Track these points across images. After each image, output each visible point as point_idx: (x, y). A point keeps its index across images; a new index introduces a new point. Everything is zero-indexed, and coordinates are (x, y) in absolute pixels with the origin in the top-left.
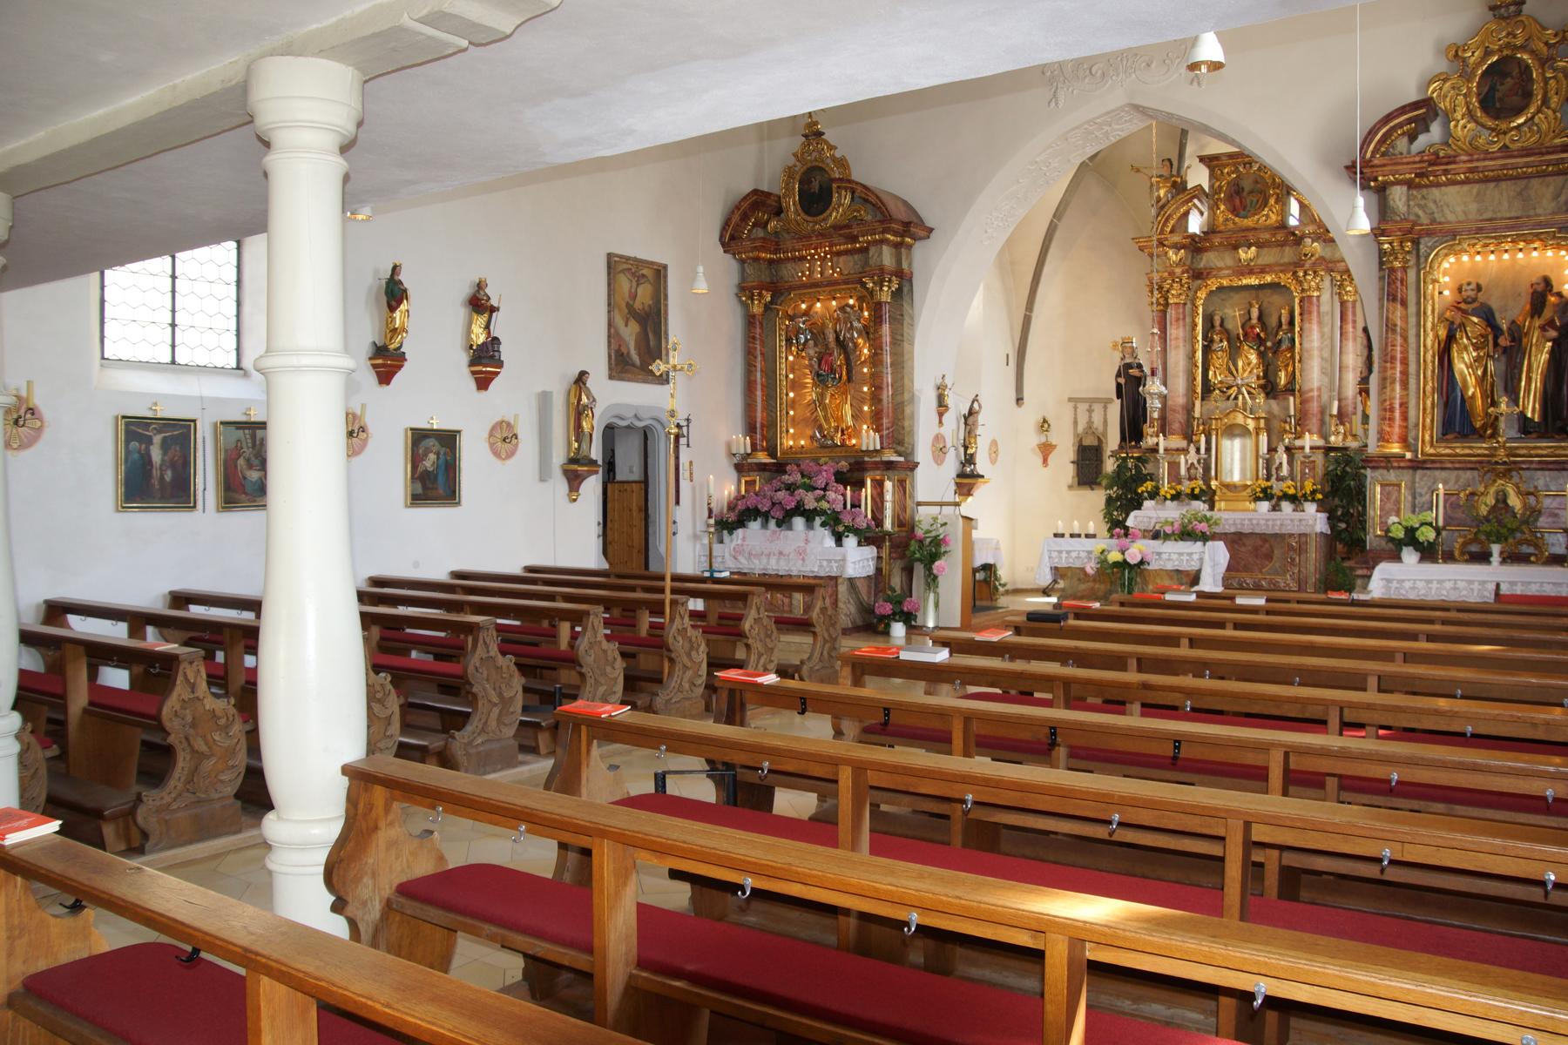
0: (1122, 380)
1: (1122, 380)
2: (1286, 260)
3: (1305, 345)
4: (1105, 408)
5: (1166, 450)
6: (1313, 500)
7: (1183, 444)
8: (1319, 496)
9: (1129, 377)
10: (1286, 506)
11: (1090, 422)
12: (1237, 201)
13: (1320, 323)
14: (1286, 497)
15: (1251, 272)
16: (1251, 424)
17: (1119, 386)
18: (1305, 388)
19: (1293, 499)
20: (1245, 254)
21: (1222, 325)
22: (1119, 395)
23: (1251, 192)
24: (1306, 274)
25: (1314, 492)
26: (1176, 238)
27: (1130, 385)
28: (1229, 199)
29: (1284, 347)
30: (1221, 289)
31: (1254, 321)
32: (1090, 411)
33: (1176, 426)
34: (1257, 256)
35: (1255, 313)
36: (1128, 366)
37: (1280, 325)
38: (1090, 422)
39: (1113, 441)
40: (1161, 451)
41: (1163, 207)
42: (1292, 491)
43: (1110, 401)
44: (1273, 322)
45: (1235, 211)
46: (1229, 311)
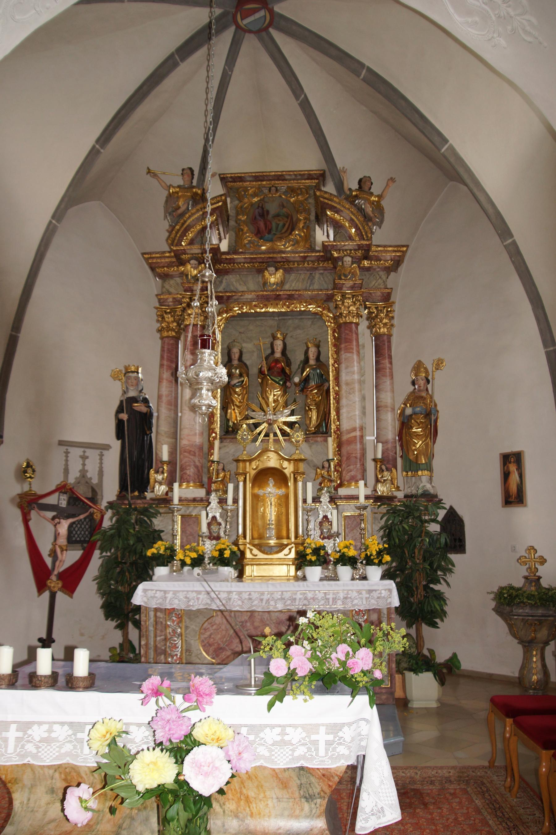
0: (124, 416)
1: (124, 416)
2: (316, 286)
3: (344, 377)
4: (101, 455)
5: (180, 500)
6: (380, 563)
7: (201, 493)
8: (387, 558)
9: (133, 413)
10: (345, 571)
11: (83, 473)
12: (262, 224)
13: (358, 352)
14: (345, 560)
15: (278, 298)
16: (288, 468)
17: (120, 424)
18: (345, 425)
19: (351, 562)
20: (274, 278)
21: (240, 359)
22: (120, 435)
23: (277, 215)
24: (344, 296)
25: (380, 553)
26: (196, 250)
27: (135, 425)
28: (254, 220)
29: (312, 383)
30: (243, 315)
31: (278, 355)
32: (84, 458)
33: (191, 471)
34: (282, 283)
35: (279, 345)
36: (133, 400)
37: (306, 360)
38: (83, 473)
39: (110, 490)
40: (176, 501)
41: (182, 215)
42: (352, 553)
43: (107, 447)
44: (297, 357)
45: (259, 234)
46: (248, 346)
